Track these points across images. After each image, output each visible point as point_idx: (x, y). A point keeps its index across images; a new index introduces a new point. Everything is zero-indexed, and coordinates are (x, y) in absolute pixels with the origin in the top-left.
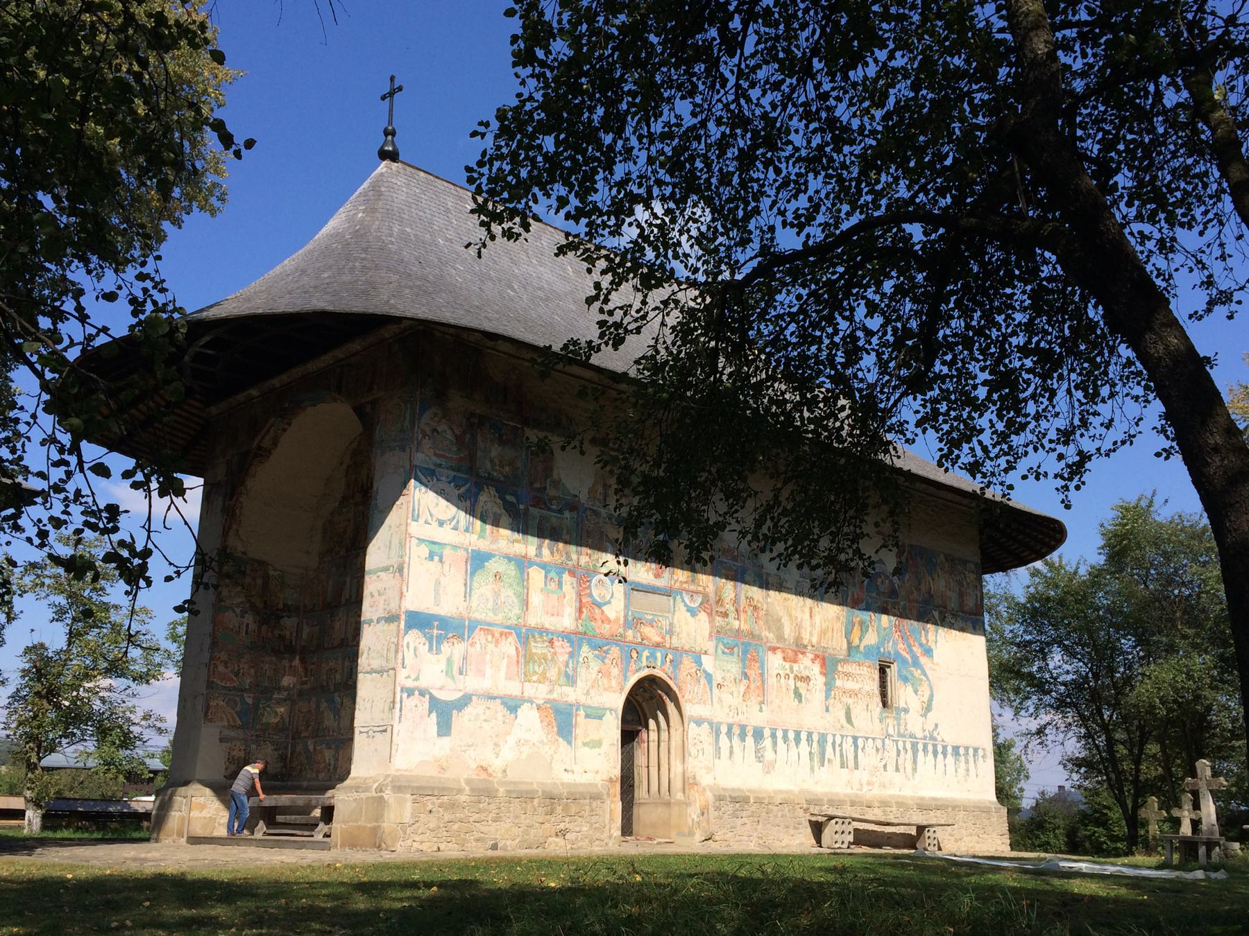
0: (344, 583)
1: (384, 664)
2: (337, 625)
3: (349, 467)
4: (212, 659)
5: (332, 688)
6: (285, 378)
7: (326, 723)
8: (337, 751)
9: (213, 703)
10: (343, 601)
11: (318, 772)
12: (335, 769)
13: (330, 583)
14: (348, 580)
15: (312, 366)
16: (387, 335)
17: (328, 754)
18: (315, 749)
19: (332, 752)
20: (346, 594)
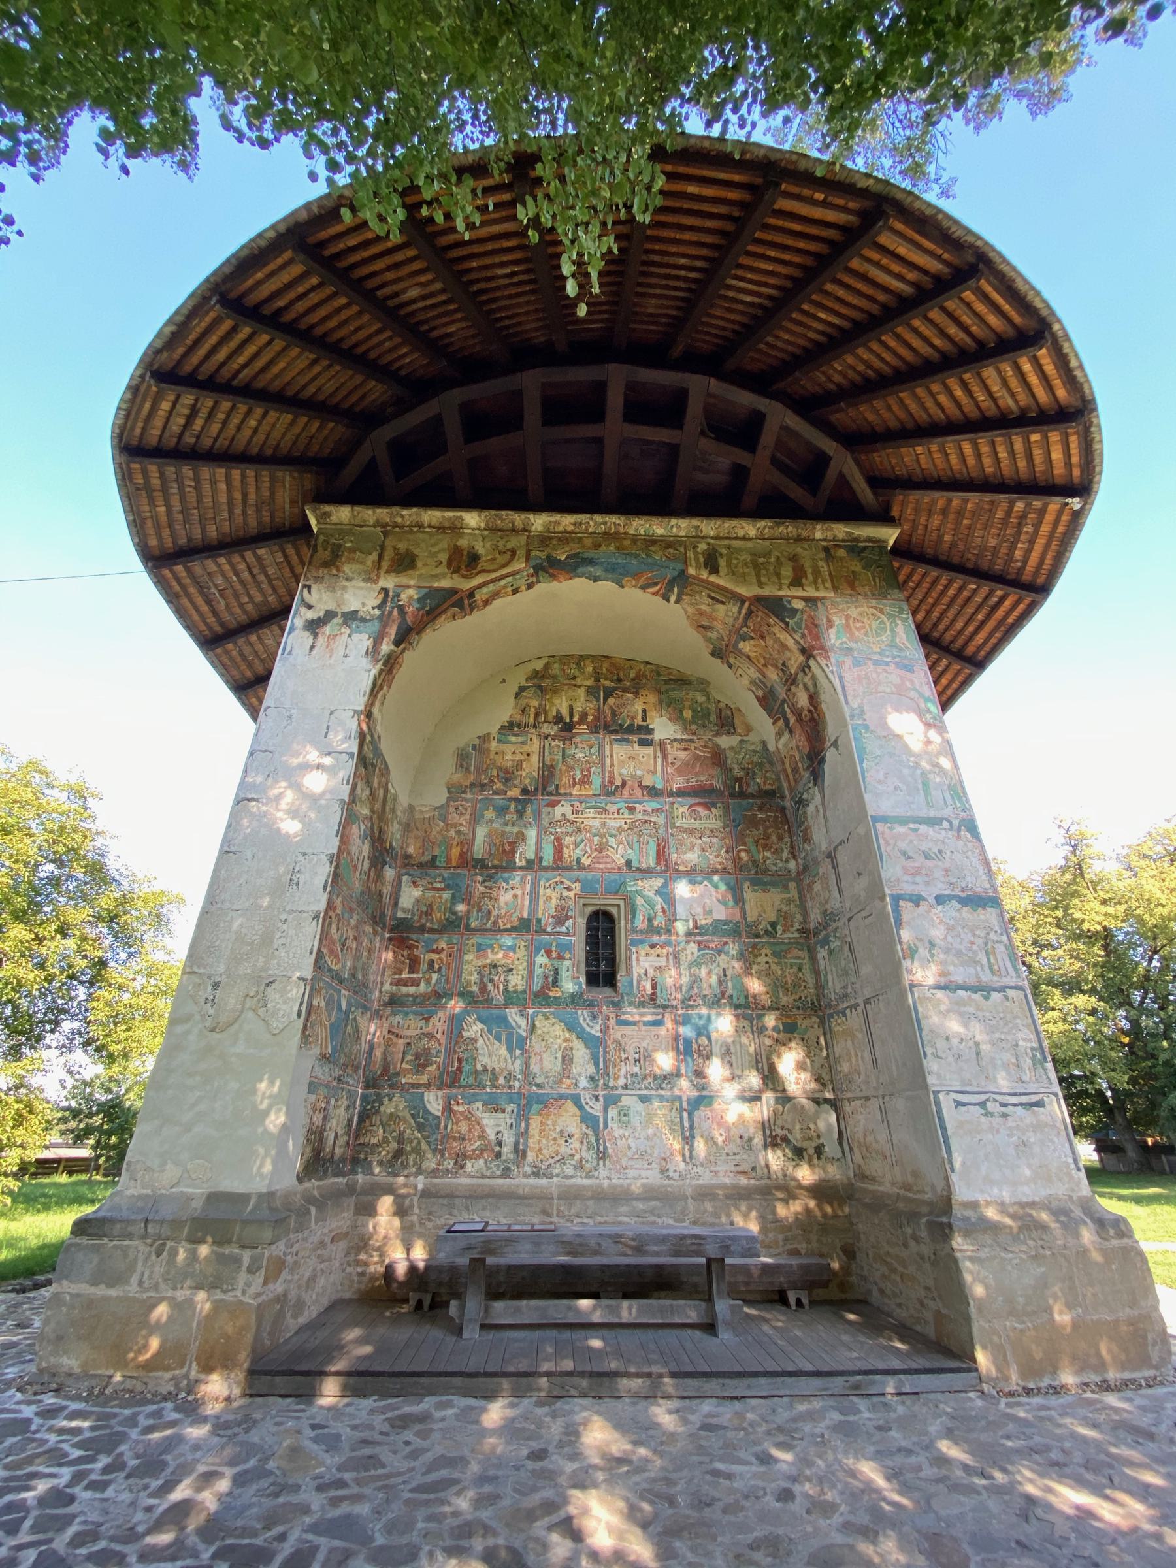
0: (521, 836)
1: (986, 977)
2: (505, 898)
3: (522, 689)
4: (330, 906)
5: (499, 998)
6: (566, 521)
7: (484, 1060)
8: (523, 1114)
9: (315, 1003)
10: (519, 862)
11: (461, 1159)
12: (520, 1153)
13: (481, 833)
14: (531, 833)
15: (641, 526)
16: (818, 535)
17: (492, 1124)
18: (448, 1109)
19: (504, 1119)
20: (528, 850)
